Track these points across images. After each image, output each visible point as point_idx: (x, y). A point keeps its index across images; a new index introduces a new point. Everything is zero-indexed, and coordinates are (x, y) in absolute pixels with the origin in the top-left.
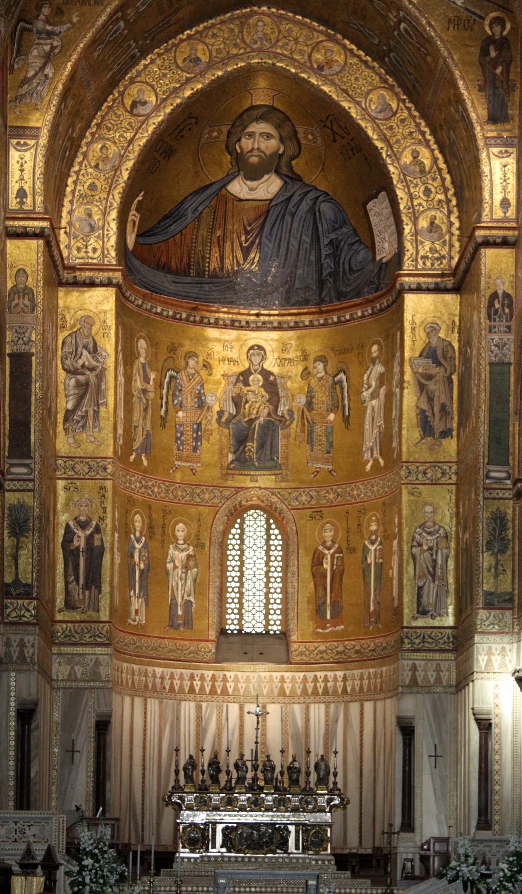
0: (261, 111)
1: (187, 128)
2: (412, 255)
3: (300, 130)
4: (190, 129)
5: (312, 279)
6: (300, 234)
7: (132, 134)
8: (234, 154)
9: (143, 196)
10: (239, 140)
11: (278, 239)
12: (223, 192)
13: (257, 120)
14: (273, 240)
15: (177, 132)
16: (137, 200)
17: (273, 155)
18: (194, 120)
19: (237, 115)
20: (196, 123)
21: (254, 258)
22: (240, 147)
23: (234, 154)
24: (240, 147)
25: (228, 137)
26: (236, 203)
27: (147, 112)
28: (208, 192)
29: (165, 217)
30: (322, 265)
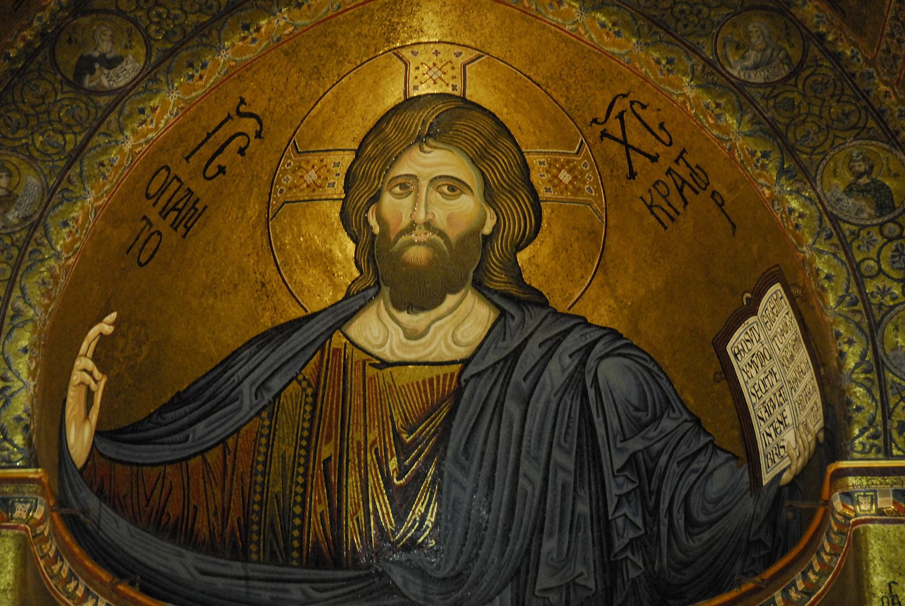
0: (428, 115)
1: (234, 145)
2: (871, 422)
3: (533, 160)
4: (242, 151)
5: (585, 562)
6: (545, 447)
7: (80, 138)
8: (363, 239)
9: (115, 324)
10: (376, 198)
11: (487, 463)
12: (338, 340)
13: (420, 140)
14: (474, 469)
15: (207, 151)
16: (94, 332)
17: (463, 240)
18: (250, 126)
19: (370, 124)
20: (258, 135)
21: (423, 518)
22: (380, 219)
23: (363, 239)
24: (380, 219)
25: (347, 188)
26: (370, 371)
27: (122, 82)
28: (298, 340)
29: (179, 400)
30: (608, 523)
